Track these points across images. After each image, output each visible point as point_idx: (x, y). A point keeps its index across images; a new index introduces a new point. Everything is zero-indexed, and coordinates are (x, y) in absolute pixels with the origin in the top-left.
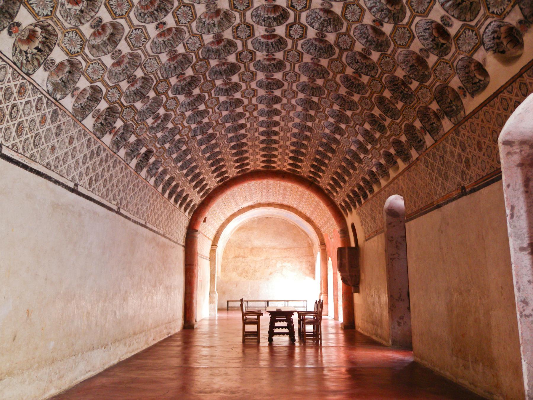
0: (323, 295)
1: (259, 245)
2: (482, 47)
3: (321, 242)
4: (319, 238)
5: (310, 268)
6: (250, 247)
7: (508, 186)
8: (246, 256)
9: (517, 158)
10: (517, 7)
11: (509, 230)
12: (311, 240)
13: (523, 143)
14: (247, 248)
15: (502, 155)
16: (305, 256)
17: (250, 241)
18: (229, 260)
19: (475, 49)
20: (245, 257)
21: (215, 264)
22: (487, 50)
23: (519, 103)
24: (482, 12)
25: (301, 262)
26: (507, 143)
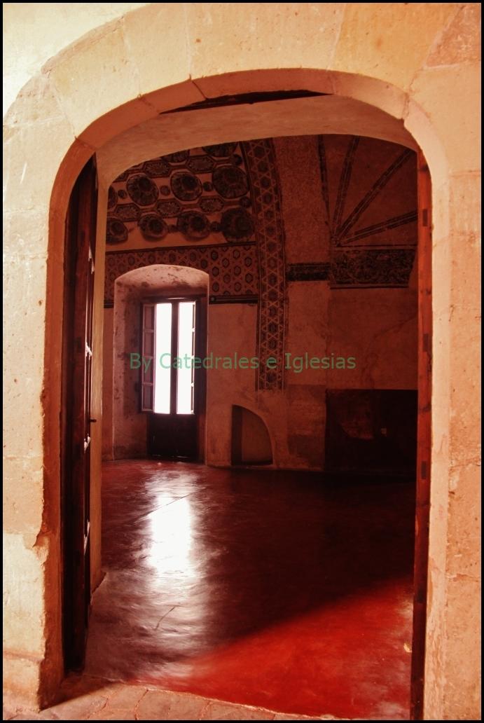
2: (136, 223)
7: (116, 313)
9: (123, 296)
10: (176, 219)
11: (114, 343)
13: (127, 286)
15: (116, 291)
19: (131, 220)
22: (138, 225)
23: (144, 266)
24: (153, 206)
26: (119, 284)
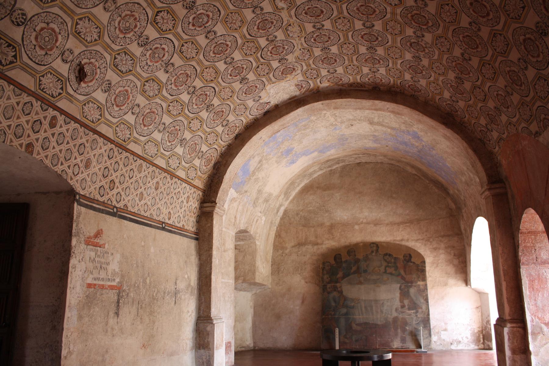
0: (509, 325)
1: (346, 218)
3: (489, 176)
4: (483, 165)
5: (456, 262)
6: (328, 224)
8: (319, 241)
12: (455, 201)
14: (322, 225)
16: (443, 236)
17: (327, 211)
18: (287, 251)
20: (317, 244)
21: (210, 248)
25: (435, 249)
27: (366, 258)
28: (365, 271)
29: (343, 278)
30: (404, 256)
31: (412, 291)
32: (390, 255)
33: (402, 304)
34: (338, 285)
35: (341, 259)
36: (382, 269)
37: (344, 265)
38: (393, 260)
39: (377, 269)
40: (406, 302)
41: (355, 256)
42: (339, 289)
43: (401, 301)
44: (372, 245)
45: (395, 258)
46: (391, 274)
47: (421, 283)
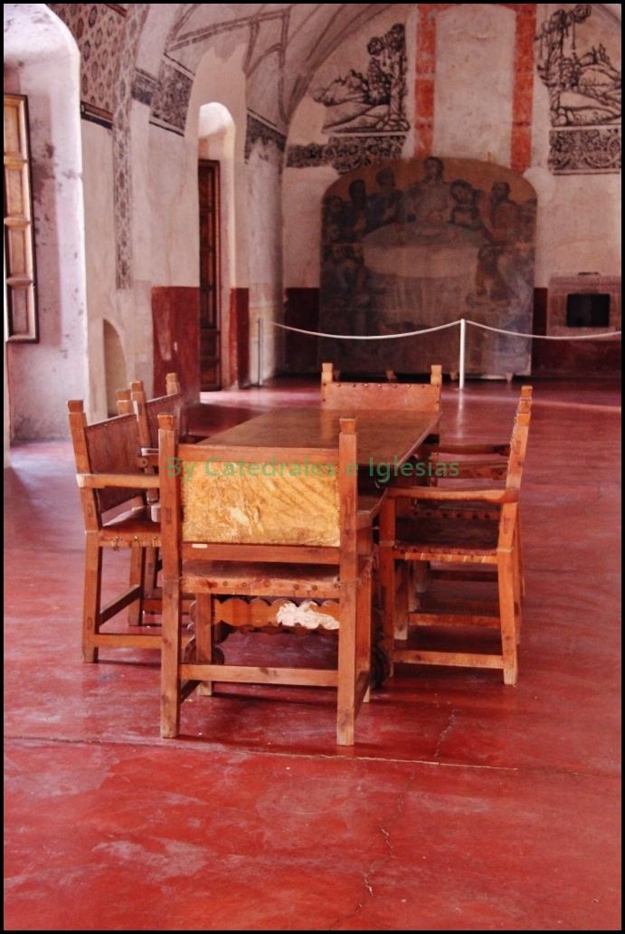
27: (415, 191)
28: (412, 218)
29: (366, 231)
30: (493, 189)
31: (503, 261)
32: (464, 184)
33: (479, 288)
34: (355, 246)
35: (364, 190)
36: (447, 215)
37: (369, 204)
38: (470, 196)
39: (436, 213)
40: (489, 284)
41: (394, 184)
42: (357, 255)
43: (480, 282)
44: (430, 162)
45: (476, 194)
46: (464, 225)
47: (522, 246)
